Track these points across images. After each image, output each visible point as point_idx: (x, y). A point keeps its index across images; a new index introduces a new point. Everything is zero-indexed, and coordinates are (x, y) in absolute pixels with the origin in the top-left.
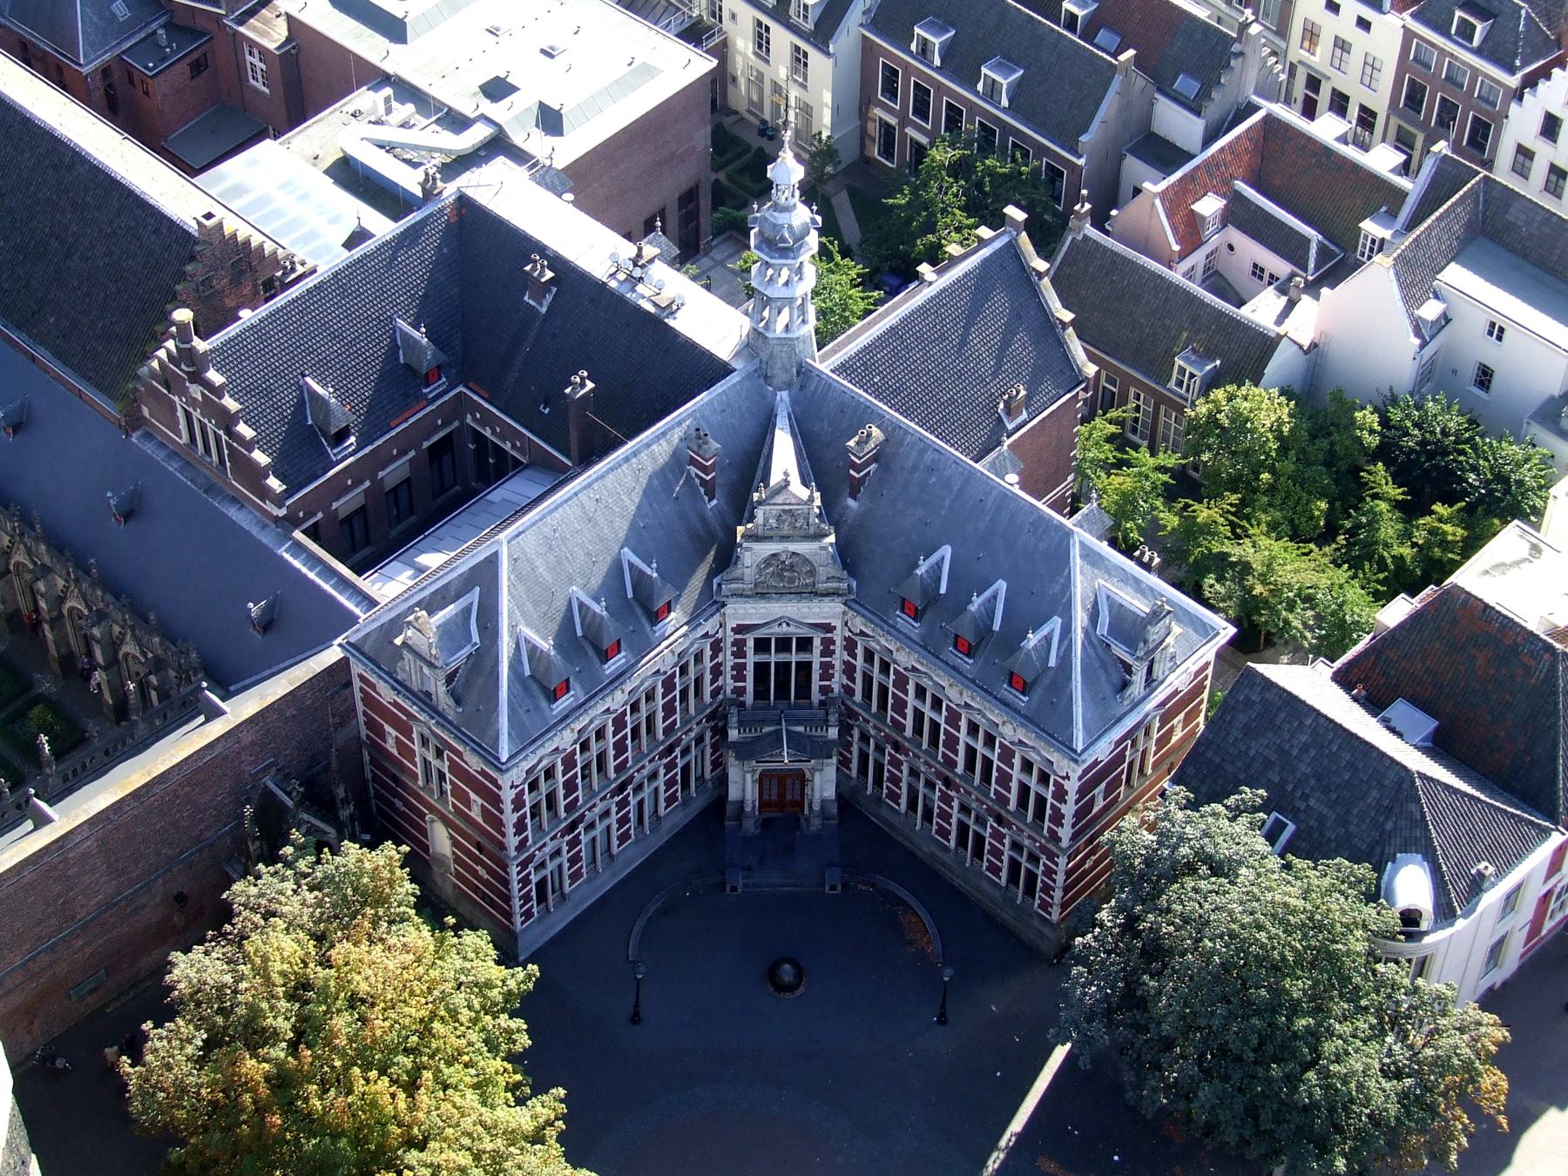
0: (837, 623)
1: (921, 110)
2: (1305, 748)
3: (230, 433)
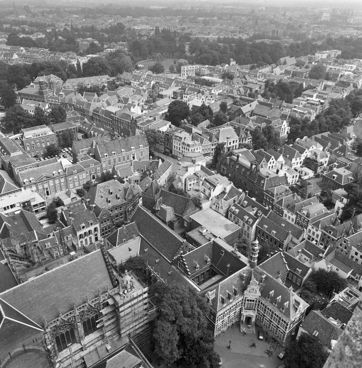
0: (258, 299)
1: (263, 235)
2: (320, 322)
3: (185, 267)
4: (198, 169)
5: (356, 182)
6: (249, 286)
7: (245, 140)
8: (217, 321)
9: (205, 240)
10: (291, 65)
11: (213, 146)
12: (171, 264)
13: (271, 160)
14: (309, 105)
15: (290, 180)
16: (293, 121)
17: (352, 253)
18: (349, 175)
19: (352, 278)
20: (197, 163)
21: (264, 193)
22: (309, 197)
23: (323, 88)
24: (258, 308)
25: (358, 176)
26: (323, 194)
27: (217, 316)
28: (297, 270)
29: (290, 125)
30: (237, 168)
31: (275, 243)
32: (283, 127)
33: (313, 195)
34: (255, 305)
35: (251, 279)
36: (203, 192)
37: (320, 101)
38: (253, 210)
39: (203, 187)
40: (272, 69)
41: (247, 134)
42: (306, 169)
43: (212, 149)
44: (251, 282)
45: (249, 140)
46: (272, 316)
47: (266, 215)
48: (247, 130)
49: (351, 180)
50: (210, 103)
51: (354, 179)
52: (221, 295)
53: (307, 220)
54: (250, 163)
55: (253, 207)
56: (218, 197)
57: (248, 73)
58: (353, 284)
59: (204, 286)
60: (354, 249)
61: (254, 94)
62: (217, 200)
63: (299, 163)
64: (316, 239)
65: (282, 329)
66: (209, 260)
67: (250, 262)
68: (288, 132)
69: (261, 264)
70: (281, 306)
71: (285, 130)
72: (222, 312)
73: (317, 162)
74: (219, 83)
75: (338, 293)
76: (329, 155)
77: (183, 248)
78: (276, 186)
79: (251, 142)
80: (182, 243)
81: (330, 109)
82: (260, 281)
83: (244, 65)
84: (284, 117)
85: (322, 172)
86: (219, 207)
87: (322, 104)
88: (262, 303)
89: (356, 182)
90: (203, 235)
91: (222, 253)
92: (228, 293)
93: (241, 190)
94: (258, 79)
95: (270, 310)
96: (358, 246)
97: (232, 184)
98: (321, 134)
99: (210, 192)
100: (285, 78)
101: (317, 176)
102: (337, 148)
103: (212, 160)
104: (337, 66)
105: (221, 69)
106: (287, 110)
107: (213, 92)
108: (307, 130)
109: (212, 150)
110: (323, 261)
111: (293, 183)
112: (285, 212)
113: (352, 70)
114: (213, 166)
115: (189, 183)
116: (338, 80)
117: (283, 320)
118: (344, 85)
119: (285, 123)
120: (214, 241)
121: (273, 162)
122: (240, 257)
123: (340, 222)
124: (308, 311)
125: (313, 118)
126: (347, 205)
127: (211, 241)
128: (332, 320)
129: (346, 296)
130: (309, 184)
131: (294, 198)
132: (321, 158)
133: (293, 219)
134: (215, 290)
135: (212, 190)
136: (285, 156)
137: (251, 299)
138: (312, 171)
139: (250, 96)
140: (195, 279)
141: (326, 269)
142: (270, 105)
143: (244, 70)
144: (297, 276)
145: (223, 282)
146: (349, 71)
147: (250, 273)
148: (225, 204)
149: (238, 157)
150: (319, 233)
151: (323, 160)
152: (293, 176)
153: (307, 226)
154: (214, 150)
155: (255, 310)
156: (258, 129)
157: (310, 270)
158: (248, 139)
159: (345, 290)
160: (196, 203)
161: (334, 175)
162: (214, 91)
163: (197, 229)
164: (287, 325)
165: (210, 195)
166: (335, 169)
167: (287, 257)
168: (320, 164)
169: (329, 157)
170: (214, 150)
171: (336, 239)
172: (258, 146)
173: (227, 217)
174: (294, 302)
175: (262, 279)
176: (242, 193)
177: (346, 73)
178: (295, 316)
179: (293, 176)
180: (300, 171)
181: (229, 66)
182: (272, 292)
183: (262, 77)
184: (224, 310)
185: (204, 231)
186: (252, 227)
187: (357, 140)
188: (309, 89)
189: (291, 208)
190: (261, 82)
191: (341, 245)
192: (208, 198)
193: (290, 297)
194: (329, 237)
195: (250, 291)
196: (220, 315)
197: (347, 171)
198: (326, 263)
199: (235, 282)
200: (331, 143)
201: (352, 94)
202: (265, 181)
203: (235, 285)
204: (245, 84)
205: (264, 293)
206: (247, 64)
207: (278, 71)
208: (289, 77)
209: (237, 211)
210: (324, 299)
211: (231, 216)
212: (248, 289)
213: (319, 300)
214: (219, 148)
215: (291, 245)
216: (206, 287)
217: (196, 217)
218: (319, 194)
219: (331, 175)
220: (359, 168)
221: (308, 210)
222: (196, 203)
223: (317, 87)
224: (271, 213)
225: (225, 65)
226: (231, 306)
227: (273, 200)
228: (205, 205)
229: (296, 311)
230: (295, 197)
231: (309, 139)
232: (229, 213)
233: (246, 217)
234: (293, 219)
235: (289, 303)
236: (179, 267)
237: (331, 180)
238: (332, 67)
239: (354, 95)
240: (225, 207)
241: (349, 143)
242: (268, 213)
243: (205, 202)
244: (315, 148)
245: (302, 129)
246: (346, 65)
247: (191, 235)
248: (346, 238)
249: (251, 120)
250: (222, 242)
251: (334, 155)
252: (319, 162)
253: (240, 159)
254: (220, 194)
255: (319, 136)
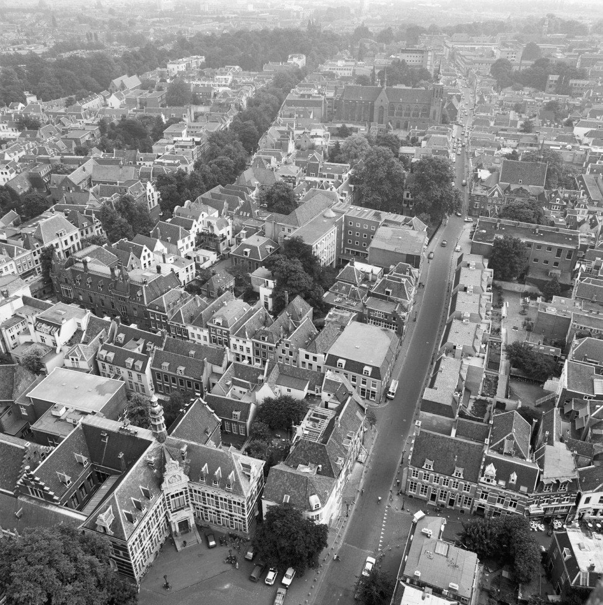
0: (187, 487)
1: (167, 380)
2: (287, 480)
3: (43, 490)
4: (19, 303)
5: (277, 252)
6: (165, 473)
7: (92, 231)
8: (133, 554)
9: (69, 427)
10: (134, 89)
11: (35, 255)
12: (15, 496)
13: (144, 254)
14: (179, 148)
15: (183, 277)
16: (162, 181)
17: (302, 358)
18: (266, 243)
19: (311, 394)
20: (12, 296)
21: (148, 310)
22: (220, 294)
23: (193, 119)
24: (192, 500)
25: (279, 241)
26: (239, 282)
27: (129, 548)
28: (234, 415)
29: (158, 187)
30: (89, 282)
31: (189, 385)
32: (148, 193)
33: (224, 290)
34: (187, 498)
35: (165, 462)
36: (41, 341)
37: (193, 139)
38: (138, 345)
39: (38, 334)
40: (105, 100)
41: (91, 220)
42: (203, 253)
43: (36, 261)
44: (166, 466)
45: (99, 229)
46: (217, 503)
47: (161, 346)
48: (89, 212)
49: (270, 251)
50: (8, 179)
51: (273, 248)
52: (124, 511)
53: (226, 332)
54: (109, 268)
55: (136, 340)
56: (70, 343)
57: (64, 114)
58: (314, 403)
59: (89, 508)
60: (303, 352)
61: (84, 149)
62: (70, 347)
63: (190, 245)
64: (247, 355)
65: (238, 516)
66: (84, 459)
67: (155, 435)
68: (159, 200)
69: (174, 431)
70: (224, 483)
71: (153, 198)
72: (135, 536)
73: (215, 236)
74: (14, 140)
75: (299, 424)
76: (229, 221)
77: (29, 458)
78: (163, 294)
79: (103, 231)
80: (23, 452)
81: (212, 149)
82: (181, 458)
83: (53, 101)
84: (145, 176)
85: (228, 249)
86: (77, 360)
87: (198, 143)
88: (195, 491)
89: (277, 252)
90: (62, 420)
91: (104, 438)
92: (134, 501)
93: (107, 319)
94: (85, 121)
95: (212, 496)
96: (307, 344)
97: (89, 313)
98: (209, 192)
99: (52, 338)
100: (129, 112)
101: (222, 258)
102: (238, 208)
103: (42, 280)
104: (205, 80)
105: (10, 114)
106: (147, 163)
107: (7, 158)
108: (187, 190)
109: (37, 263)
110: (266, 385)
111: (190, 280)
112: (190, 329)
113: (228, 84)
114: (47, 291)
115: (10, 335)
116: (212, 102)
117: (235, 502)
118: (223, 107)
119: (149, 186)
120: (83, 425)
121: (149, 255)
122: (136, 433)
123: (274, 317)
124: (266, 471)
125: (190, 168)
126: (276, 289)
127: (78, 426)
128: (303, 468)
129: (311, 423)
130: (214, 274)
131: (197, 305)
132: (220, 229)
133: (205, 337)
134: (110, 508)
135: (56, 334)
136: (164, 240)
137: (177, 492)
138: (212, 252)
139: (79, 152)
140: (70, 501)
141: (273, 396)
142: (116, 162)
143: (55, 109)
144: (236, 423)
145: (119, 487)
146: (225, 86)
147: (161, 451)
148: (85, 352)
149: (85, 263)
150: (249, 345)
151: (224, 231)
152: (187, 268)
153: (229, 340)
154: (39, 261)
155: (188, 506)
156: (108, 207)
157: (253, 407)
158: (97, 227)
159: (307, 416)
160: (33, 367)
161: (247, 250)
162: (10, 156)
163: (48, 412)
164: (243, 506)
165: (55, 344)
166: (244, 240)
167: (212, 402)
168: (221, 238)
169: (230, 224)
170: (39, 261)
171: (275, 345)
172: (116, 235)
173: (97, 372)
174: (242, 468)
175: (183, 454)
176: (110, 323)
177: (221, 90)
178: (249, 488)
179: (187, 268)
180: (195, 258)
181: (26, 105)
182: (204, 467)
183: (90, 115)
184: (138, 531)
185: (62, 412)
186: (144, 373)
187: (262, 188)
188: (172, 123)
189: (196, 320)
190: (92, 125)
191: (284, 351)
192: (53, 350)
193: (233, 463)
194: (264, 346)
195: (171, 481)
196: (134, 544)
197: (261, 238)
198: (271, 387)
199: (141, 477)
200: (228, 202)
201: (237, 120)
202: (142, 291)
203: (142, 483)
204: (63, 133)
205: (194, 474)
206: (58, 98)
207: (114, 102)
208: (135, 109)
209: (111, 355)
210: (284, 440)
211: (104, 367)
212: (166, 479)
213: (278, 446)
214: (48, 256)
215: (213, 380)
216: (94, 507)
217: (41, 392)
218: (232, 284)
219: (240, 251)
220: (276, 229)
221: (222, 316)
222: (33, 367)
223: (184, 119)
224: (168, 339)
225: (18, 105)
226: (147, 519)
227: (166, 318)
228: (51, 364)
229: (249, 480)
230: (198, 301)
231: (194, 203)
232: (100, 363)
233: (130, 361)
234: (205, 337)
235: (236, 472)
236: (33, 494)
237: (244, 258)
238: (198, 83)
239: (241, 122)
240: (89, 355)
241: (253, 195)
242: (163, 341)
243: (48, 360)
244: (206, 215)
245: (180, 189)
246: (218, 77)
247: (39, 428)
248: (288, 340)
249: (91, 194)
250: (98, 421)
251: (237, 221)
252: (218, 236)
253: (89, 265)
254: (73, 337)
255: (207, 195)
